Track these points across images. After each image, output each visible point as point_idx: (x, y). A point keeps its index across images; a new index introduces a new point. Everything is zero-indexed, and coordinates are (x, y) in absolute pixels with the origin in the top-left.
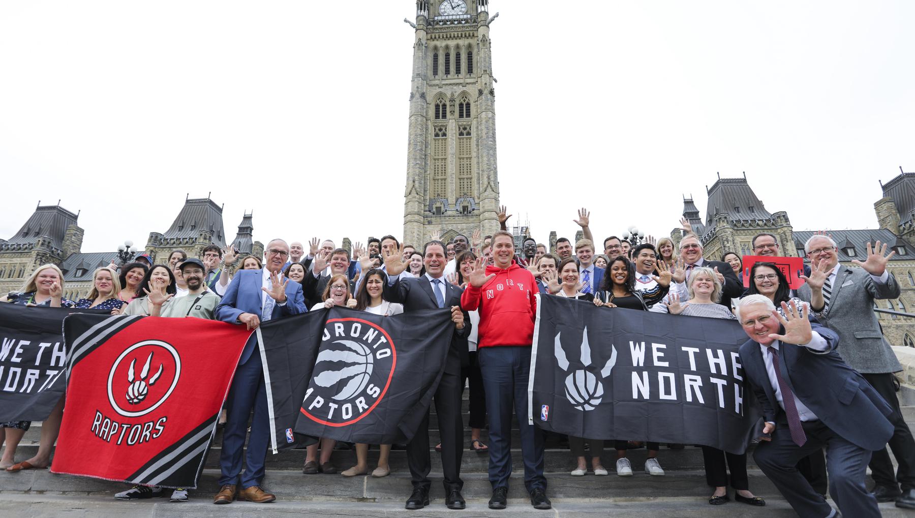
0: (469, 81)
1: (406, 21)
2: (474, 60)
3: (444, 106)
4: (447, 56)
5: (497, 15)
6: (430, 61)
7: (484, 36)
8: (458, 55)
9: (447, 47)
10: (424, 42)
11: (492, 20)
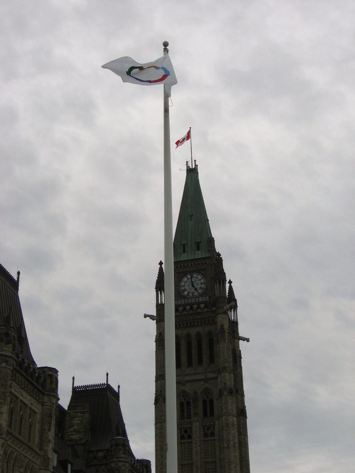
0: (210, 375)
1: (146, 316)
3: (188, 404)
9: (188, 335)
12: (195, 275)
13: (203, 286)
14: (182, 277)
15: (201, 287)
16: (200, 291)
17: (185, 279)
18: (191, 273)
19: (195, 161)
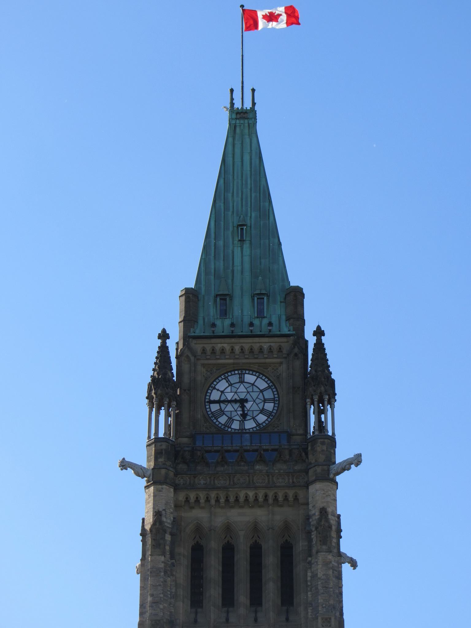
1: (124, 465)
2: (299, 569)
4: (228, 551)
5: (357, 460)
6: (182, 574)
7: (323, 512)
8: (256, 552)
9: (228, 528)
10: (168, 520)
11: (346, 466)
12: (249, 378)
13: (269, 406)
14: (217, 379)
15: (263, 408)
16: (262, 418)
17: (222, 385)
18: (242, 370)
19: (253, 90)
